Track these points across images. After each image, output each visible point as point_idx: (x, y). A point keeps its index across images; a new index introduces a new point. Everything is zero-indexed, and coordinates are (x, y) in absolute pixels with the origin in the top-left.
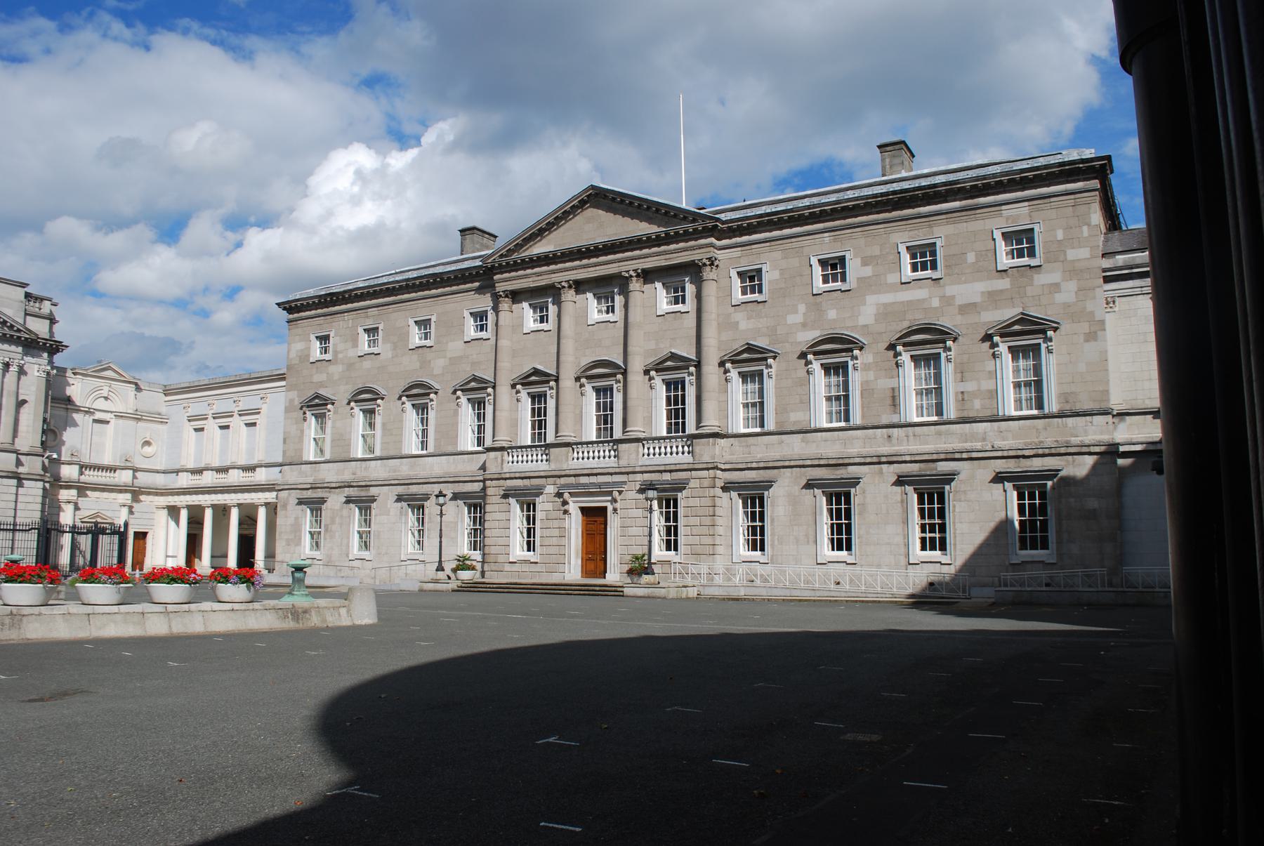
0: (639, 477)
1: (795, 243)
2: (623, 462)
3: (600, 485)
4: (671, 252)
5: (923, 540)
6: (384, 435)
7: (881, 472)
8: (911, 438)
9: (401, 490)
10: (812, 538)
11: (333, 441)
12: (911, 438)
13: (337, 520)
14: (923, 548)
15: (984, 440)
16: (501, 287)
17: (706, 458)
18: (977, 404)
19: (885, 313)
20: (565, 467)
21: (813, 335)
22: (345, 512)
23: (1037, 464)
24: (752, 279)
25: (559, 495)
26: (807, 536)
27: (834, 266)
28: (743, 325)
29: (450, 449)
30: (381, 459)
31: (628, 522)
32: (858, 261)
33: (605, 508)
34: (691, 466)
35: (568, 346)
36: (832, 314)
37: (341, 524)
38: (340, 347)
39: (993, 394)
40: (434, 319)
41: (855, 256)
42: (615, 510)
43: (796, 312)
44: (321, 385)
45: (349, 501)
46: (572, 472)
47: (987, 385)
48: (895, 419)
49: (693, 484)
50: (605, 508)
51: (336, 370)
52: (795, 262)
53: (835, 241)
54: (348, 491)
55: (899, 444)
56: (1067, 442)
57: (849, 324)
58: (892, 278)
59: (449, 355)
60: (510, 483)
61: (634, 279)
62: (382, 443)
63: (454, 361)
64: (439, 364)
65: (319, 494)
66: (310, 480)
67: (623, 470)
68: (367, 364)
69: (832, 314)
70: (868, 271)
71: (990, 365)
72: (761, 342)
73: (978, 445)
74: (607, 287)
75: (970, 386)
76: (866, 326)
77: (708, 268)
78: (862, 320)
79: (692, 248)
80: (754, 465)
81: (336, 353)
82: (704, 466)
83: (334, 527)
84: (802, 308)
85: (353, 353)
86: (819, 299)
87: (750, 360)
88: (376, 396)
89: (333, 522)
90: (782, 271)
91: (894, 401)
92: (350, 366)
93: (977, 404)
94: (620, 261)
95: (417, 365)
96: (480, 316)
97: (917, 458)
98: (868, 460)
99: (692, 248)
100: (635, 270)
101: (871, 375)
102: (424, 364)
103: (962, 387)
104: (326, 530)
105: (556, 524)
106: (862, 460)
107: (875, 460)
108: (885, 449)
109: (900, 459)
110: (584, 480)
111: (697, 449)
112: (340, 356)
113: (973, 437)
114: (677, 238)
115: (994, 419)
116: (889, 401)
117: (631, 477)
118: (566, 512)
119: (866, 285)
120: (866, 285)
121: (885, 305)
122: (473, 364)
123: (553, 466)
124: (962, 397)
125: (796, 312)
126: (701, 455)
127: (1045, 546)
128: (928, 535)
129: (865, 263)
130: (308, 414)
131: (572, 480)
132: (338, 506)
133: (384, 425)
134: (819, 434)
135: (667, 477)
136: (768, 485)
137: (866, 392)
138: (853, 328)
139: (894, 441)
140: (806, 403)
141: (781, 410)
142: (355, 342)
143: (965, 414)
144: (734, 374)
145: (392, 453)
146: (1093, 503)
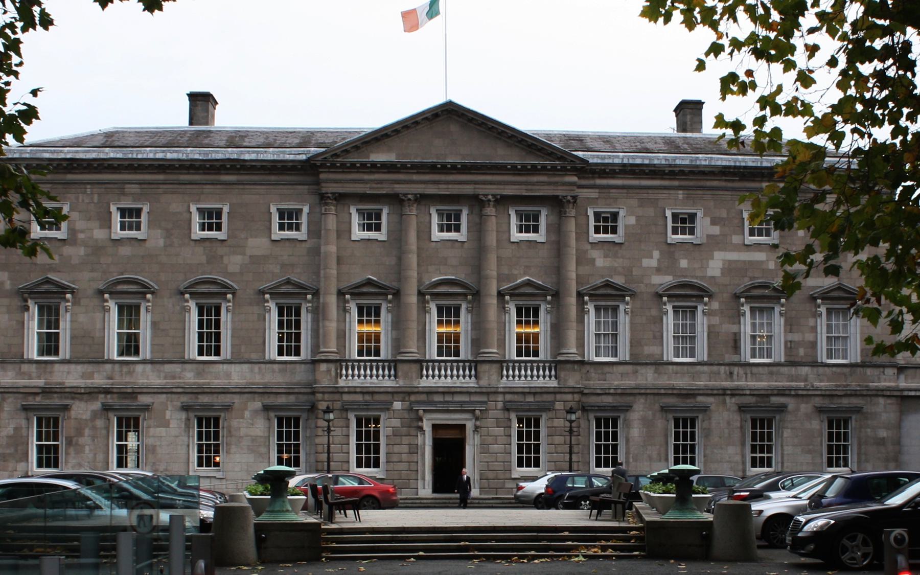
0: (500, 398)
1: (652, 195)
2: (484, 382)
3: (462, 403)
4: (533, 184)
5: (200, 459)
6: (154, 336)
7: (724, 402)
8: (749, 375)
9: (185, 399)
10: (663, 456)
11: (72, 338)
12: (749, 375)
13: (87, 432)
14: (200, 464)
15: (806, 380)
16: (331, 188)
17: (571, 382)
18: (802, 352)
19: (730, 268)
20: (416, 384)
21: (667, 279)
22: (100, 423)
23: (845, 402)
24: (608, 223)
25: (410, 410)
26: (659, 454)
27: (685, 222)
28: (600, 262)
29: (254, 357)
30: (152, 362)
31: (490, 440)
32: (708, 220)
33: (464, 426)
34: (557, 390)
35: (413, 259)
36: (684, 263)
37: (93, 438)
38: (80, 225)
39: (814, 345)
40: (226, 209)
41: (705, 215)
42: (476, 429)
43: (651, 257)
44: (52, 269)
45: (107, 408)
46: (426, 390)
47: (809, 337)
48: (735, 358)
49: (559, 406)
50: (464, 426)
51: (76, 253)
52: (650, 212)
53: (687, 198)
54: (110, 400)
55: (738, 380)
56: (867, 386)
57: (699, 274)
58: (736, 239)
59: (249, 252)
60: (346, 397)
61: (492, 203)
62: (152, 345)
63: (256, 260)
64: (234, 262)
65: (56, 401)
66: (41, 382)
67: (484, 390)
68: (125, 251)
69: (684, 263)
70: (716, 230)
71: (811, 322)
72: (619, 280)
73: (802, 384)
74: (451, 206)
75: (796, 337)
76: (713, 277)
77: (571, 206)
78: (710, 273)
79: (555, 184)
80: (612, 391)
81: (72, 231)
82: (571, 390)
83: (81, 440)
84: (656, 254)
85: (99, 234)
86: (672, 249)
87: (608, 296)
88: (144, 290)
89: (80, 433)
90: (638, 218)
91: (736, 346)
92: (97, 249)
93: (802, 352)
94: (476, 183)
95: (204, 259)
96: (289, 218)
97: (755, 392)
98: (715, 392)
99: (555, 184)
100: (494, 196)
101: (716, 320)
102: (214, 259)
103: (791, 337)
104: (69, 442)
105: (405, 440)
106: (710, 392)
107: (721, 392)
108: (727, 384)
109: (741, 392)
110: (437, 398)
111: (562, 374)
112: (81, 236)
113: (797, 378)
114: (534, 170)
115: (814, 364)
116: (732, 344)
117: (492, 398)
118: (421, 429)
119: (714, 243)
120: (714, 243)
121: (730, 262)
122: (283, 266)
123: (401, 383)
124: (790, 347)
125: (651, 257)
126: (566, 380)
127: (377, 465)
128: (758, 455)
129: (714, 222)
130: (30, 303)
131: (423, 397)
132: (87, 416)
133: (154, 324)
134: (670, 367)
135: (530, 399)
136: (628, 408)
137: (712, 333)
138: (703, 278)
139: (735, 377)
140: (659, 339)
141: (635, 343)
142: (106, 223)
143: (792, 359)
144: (590, 307)
145: (168, 356)
146: (883, 433)
